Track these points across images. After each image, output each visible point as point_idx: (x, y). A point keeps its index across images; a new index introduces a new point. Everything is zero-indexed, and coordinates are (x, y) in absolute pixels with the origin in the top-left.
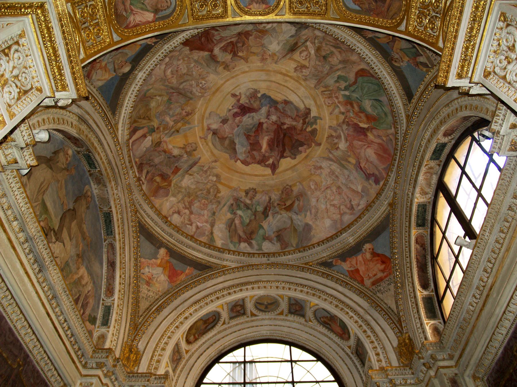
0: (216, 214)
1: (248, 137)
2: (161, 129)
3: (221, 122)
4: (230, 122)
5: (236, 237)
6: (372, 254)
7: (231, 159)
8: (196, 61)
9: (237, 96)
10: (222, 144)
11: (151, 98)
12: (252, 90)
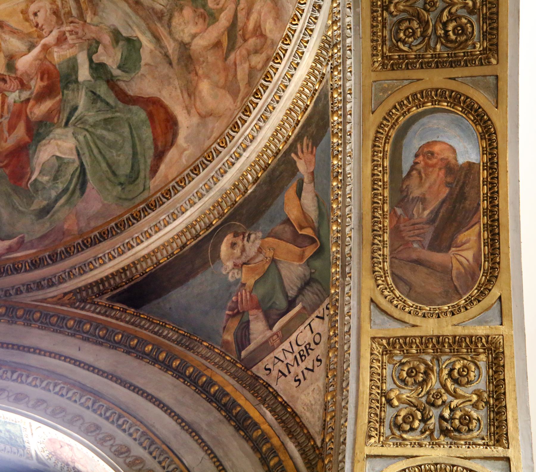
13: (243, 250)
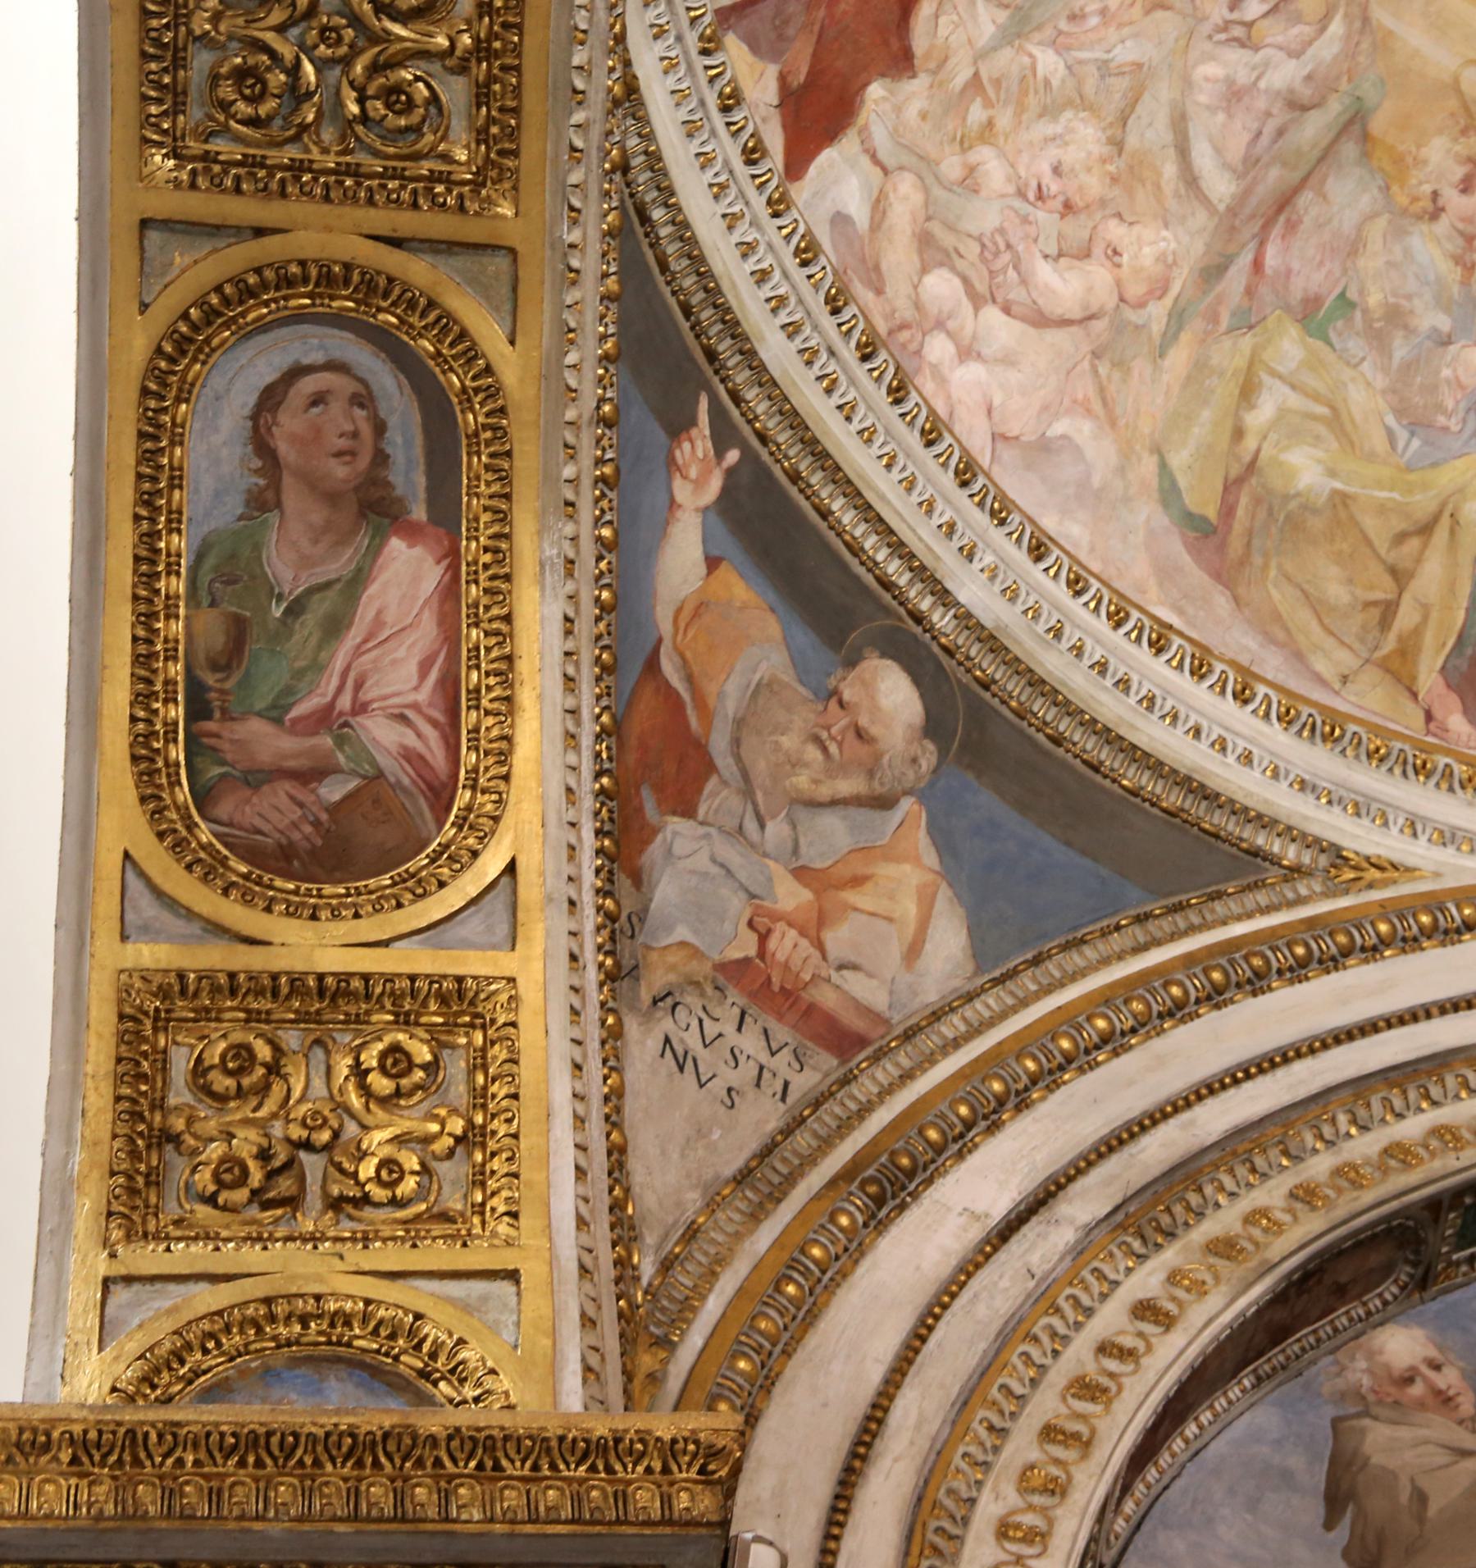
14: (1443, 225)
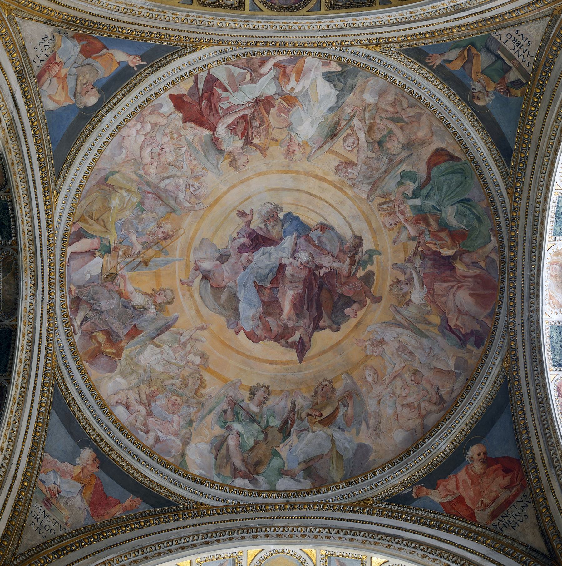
0: (194, 424)
1: (260, 289)
2: (121, 252)
3: (217, 260)
4: (232, 260)
5: (229, 468)
6: (484, 462)
7: (229, 327)
8: (189, 144)
9: (247, 215)
10: (217, 298)
11: (114, 189)
12: (271, 207)
13: (480, 92)
14: (156, 229)
